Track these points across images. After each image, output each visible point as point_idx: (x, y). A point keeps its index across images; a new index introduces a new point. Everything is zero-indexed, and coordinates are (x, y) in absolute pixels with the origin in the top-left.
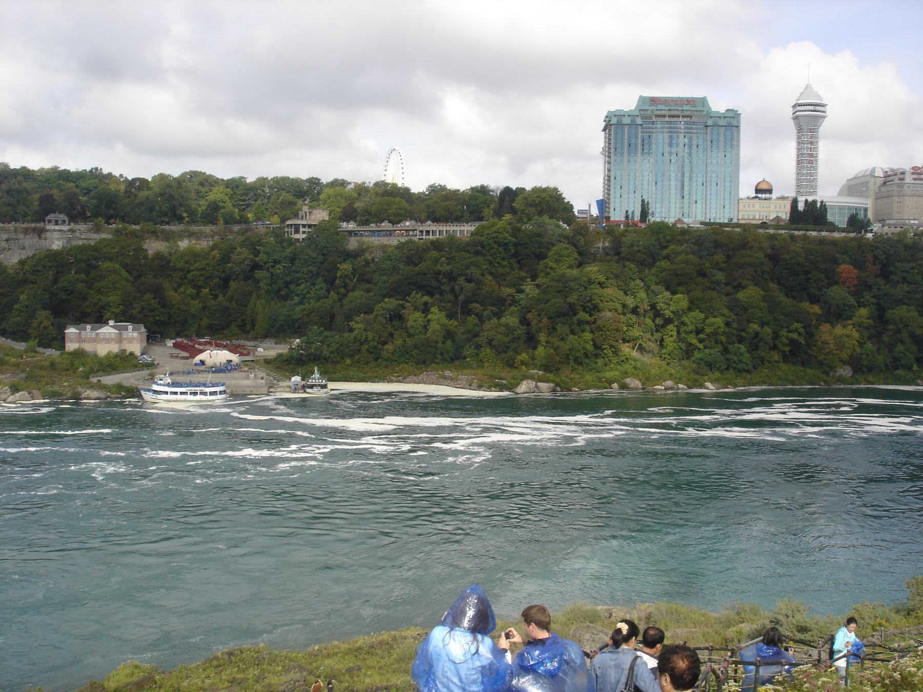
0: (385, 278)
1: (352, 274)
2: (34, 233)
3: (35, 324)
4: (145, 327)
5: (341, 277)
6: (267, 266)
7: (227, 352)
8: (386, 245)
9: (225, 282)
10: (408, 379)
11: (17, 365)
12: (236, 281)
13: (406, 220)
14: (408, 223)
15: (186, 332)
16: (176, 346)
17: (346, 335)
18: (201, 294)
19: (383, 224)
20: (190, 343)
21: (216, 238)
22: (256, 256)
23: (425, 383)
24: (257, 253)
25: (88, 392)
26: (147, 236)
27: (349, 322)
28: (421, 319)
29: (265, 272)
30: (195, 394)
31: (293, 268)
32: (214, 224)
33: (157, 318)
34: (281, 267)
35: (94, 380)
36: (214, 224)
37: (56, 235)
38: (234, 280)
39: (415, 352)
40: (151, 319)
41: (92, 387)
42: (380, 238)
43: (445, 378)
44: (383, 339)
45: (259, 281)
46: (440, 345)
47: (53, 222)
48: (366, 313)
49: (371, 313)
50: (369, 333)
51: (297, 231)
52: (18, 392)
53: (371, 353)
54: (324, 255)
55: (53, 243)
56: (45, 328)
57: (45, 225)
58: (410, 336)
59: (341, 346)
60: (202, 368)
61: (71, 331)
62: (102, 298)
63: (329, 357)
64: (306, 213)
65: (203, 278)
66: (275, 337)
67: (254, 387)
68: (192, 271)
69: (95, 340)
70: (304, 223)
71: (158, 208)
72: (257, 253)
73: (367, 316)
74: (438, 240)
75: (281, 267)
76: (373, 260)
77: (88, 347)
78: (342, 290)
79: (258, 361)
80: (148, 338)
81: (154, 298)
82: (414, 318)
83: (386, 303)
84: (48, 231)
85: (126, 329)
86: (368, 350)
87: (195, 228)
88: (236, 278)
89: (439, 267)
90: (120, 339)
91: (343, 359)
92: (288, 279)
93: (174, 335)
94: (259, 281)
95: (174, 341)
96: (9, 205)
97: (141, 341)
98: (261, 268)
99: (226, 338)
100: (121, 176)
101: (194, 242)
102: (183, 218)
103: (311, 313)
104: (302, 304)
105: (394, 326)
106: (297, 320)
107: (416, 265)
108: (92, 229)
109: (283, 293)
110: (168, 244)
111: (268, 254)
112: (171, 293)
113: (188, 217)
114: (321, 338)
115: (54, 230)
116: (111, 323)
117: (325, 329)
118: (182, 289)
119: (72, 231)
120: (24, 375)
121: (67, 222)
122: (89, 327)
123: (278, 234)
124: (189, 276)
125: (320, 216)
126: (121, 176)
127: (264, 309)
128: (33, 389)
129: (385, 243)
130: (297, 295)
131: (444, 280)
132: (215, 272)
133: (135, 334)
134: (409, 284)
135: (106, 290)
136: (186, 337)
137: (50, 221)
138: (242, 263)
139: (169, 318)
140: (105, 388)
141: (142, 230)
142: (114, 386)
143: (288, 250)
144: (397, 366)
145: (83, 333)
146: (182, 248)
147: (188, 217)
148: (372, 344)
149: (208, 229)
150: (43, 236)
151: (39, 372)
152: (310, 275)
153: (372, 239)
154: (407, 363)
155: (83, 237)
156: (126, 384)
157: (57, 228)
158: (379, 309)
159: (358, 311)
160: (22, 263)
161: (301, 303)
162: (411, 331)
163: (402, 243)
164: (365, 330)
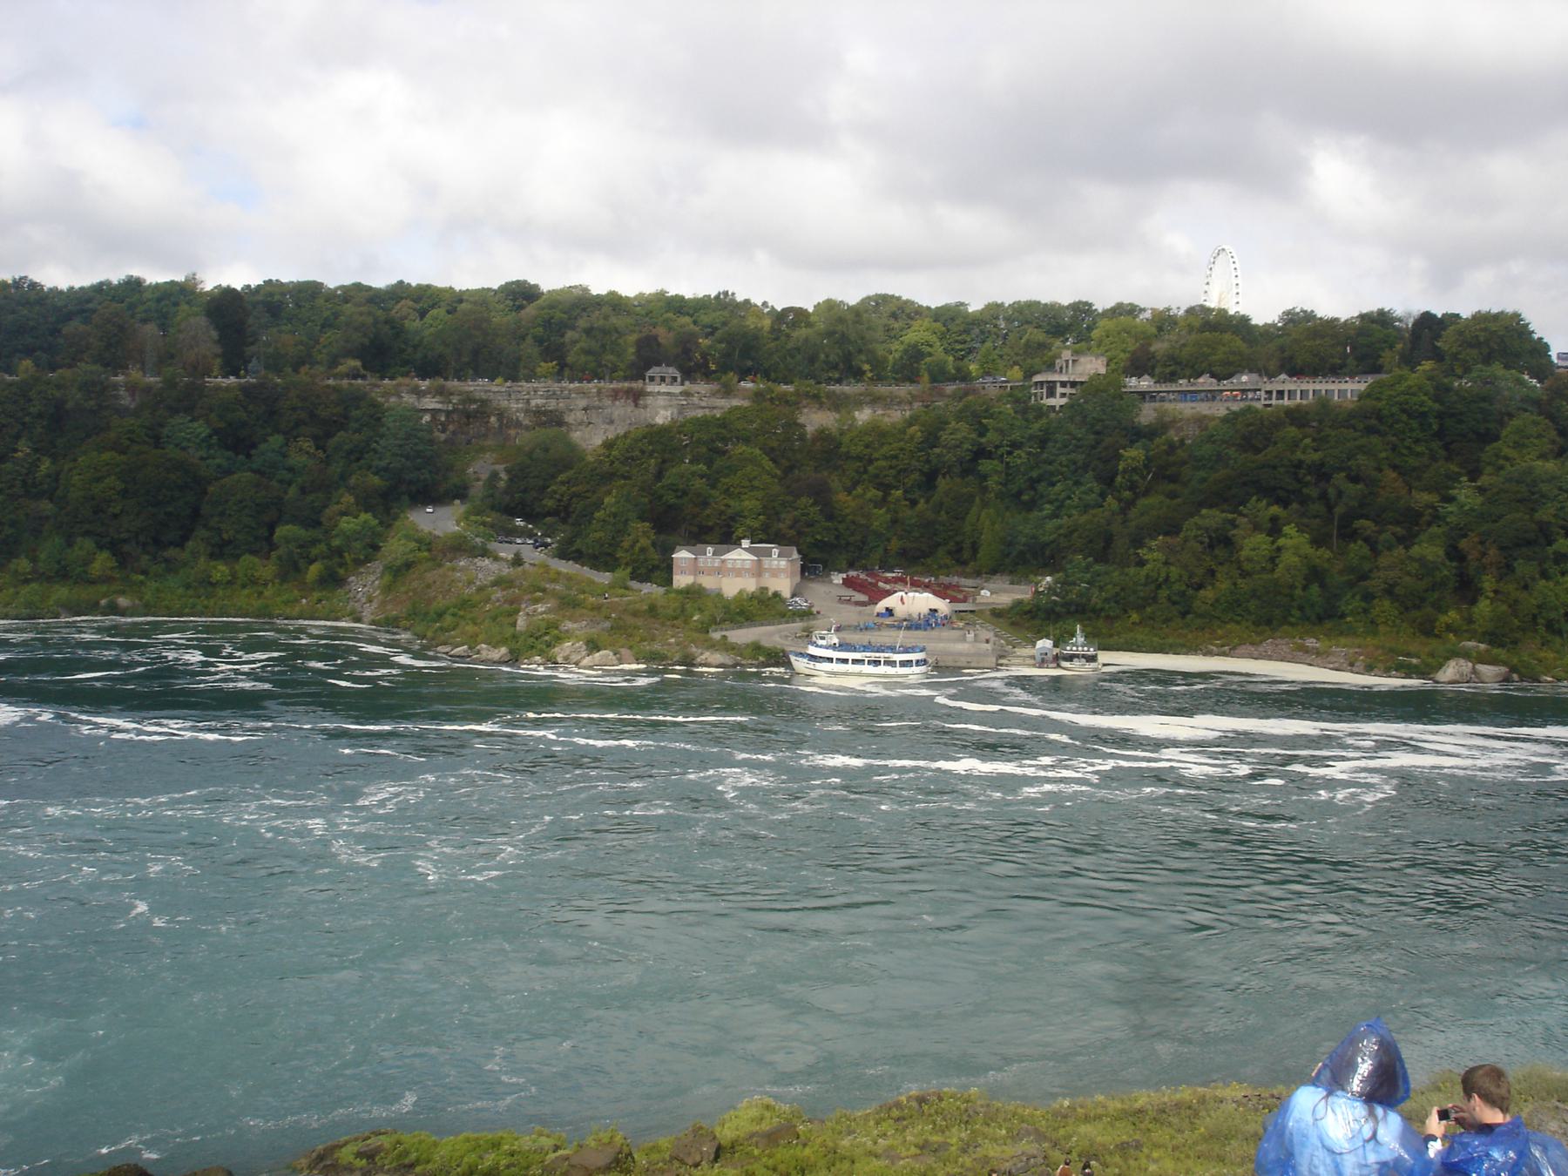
0: (1202, 474)
1: (1146, 466)
2: (627, 398)
3: (626, 544)
4: (799, 552)
5: (1125, 471)
6: (999, 453)
7: (931, 595)
8: (1205, 416)
9: (929, 480)
10: (1241, 650)
11: (597, 608)
12: (948, 476)
13: (1242, 373)
14: (1244, 378)
16: (848, 583)
17: (1132, 570)
18: (890, 499)
19: (1201, 380)
20: (869, 580)
21: (916, 405)
22: (982, 435)
23: (1270, 658)
25: (707, 654)
26: (805, 402)
28: (1265, 546)
29: (996, 462)
30: (876, 663)
31: (1045, 455)
32: (914, 382)
33: (818, 537)
34: (1023, 455)
35: (716, 636)
36: (912, 381)
37: (661, 401)
38: (944, 478)
39: (1253, 605)
40: (809, 539)
41: (713, 646)
42: (1193, 405)
43: (1306, 651)
44: (1196, 580)
45: (984, 477)
46: (1298, 592)
47: (658, 379)
48: (1166, 534)
49: (1177, 533)
50: (1172, 568)
51: (1051, 394)
52: (599, 651)
53: (1174, 603)
54: (1097, 433)
55: (657, 413)
56: (643, 550)
57: (645, 384)
58: (1245, 574)
59: (1123, 589)
60: (888, 621)
61: (682, 555)
62: (732, 503)
63: (1102, 609)
64: (1067, 361)
65: (893, 472)
66: (1011, 572)
68: (877, 459)
69: (720, 571)
70: (1065, 378)
71: (822, 356)
73: (1168, 539)
74: (1299, 406)
75: (1023, 455)
76: (1182, 441)
77: (708, 582)
78: (1127, 494)
79: (981, 611)
80: (803, 569)
81: (812, 505)
82: (1254, 545)
83: (1202, 517)
84: (650, 394)
86: (1169, 599)
87: (882, 389)
88: (948, 472)
89: (1299, 455)
90: (758, 571)
91: (1125, 611)
92: (1034, 474)
93: (844, 565)
94: (984, 477)
95: (844, 576)
96: (588, 352)
97: (792, 574)
98: (990, 456)
99: (930, 573)
100: (765, 304)
101: (880, 412)
102: (864, 373)
103: (1071, 533)
105: (1216, 557)
106: (1048, 545)
107: (1258, 451)
108: (718, 391)
109: (1025, 497)
110: (837, 416)
111: (1001, 431)
113: (871, 371)
114: (1088, 575)
115: (659, 393)
116: (746, 543)
117: (1096, 561)
118: (859, 490)
119: (687, 394)
120: (607, 624)
121: (679, 380)
122: (710, 549)
123: (1019, 399)
124: (870, 468)
125: (1091, 366)
126: (765, 304)
127: (993, 523)
129: (1205, 412)
130: (1050, 502)
131: (1309, 478)
132: (914, 463)
133: (783, 563)
134: (1245, 484)
135: (737, 491)
136: (864, 568)
137: (652, 379)
138: (958, 447)
139: (837, 537)
140: (733, 649)
141: (797, 393)
143: (1036, 426)
144: (1220, 627)
145: (701, 559)
146: (860, 423)
147: (871, 371)
148: (1176, 587)
149: (903, 390)
151: (630, 620)
152: (1072, 467)
153: (1180, 406)
154: (1238, 623)
155: (703, 404)
156: (766, 643)
157: (663, 388)
158: (1190, 527)
159: (1154, 530)
160: (609, 445)
161: (1055, 515)
162: (1247, 566)
163: (1234, 413)
164: (1166, 563)
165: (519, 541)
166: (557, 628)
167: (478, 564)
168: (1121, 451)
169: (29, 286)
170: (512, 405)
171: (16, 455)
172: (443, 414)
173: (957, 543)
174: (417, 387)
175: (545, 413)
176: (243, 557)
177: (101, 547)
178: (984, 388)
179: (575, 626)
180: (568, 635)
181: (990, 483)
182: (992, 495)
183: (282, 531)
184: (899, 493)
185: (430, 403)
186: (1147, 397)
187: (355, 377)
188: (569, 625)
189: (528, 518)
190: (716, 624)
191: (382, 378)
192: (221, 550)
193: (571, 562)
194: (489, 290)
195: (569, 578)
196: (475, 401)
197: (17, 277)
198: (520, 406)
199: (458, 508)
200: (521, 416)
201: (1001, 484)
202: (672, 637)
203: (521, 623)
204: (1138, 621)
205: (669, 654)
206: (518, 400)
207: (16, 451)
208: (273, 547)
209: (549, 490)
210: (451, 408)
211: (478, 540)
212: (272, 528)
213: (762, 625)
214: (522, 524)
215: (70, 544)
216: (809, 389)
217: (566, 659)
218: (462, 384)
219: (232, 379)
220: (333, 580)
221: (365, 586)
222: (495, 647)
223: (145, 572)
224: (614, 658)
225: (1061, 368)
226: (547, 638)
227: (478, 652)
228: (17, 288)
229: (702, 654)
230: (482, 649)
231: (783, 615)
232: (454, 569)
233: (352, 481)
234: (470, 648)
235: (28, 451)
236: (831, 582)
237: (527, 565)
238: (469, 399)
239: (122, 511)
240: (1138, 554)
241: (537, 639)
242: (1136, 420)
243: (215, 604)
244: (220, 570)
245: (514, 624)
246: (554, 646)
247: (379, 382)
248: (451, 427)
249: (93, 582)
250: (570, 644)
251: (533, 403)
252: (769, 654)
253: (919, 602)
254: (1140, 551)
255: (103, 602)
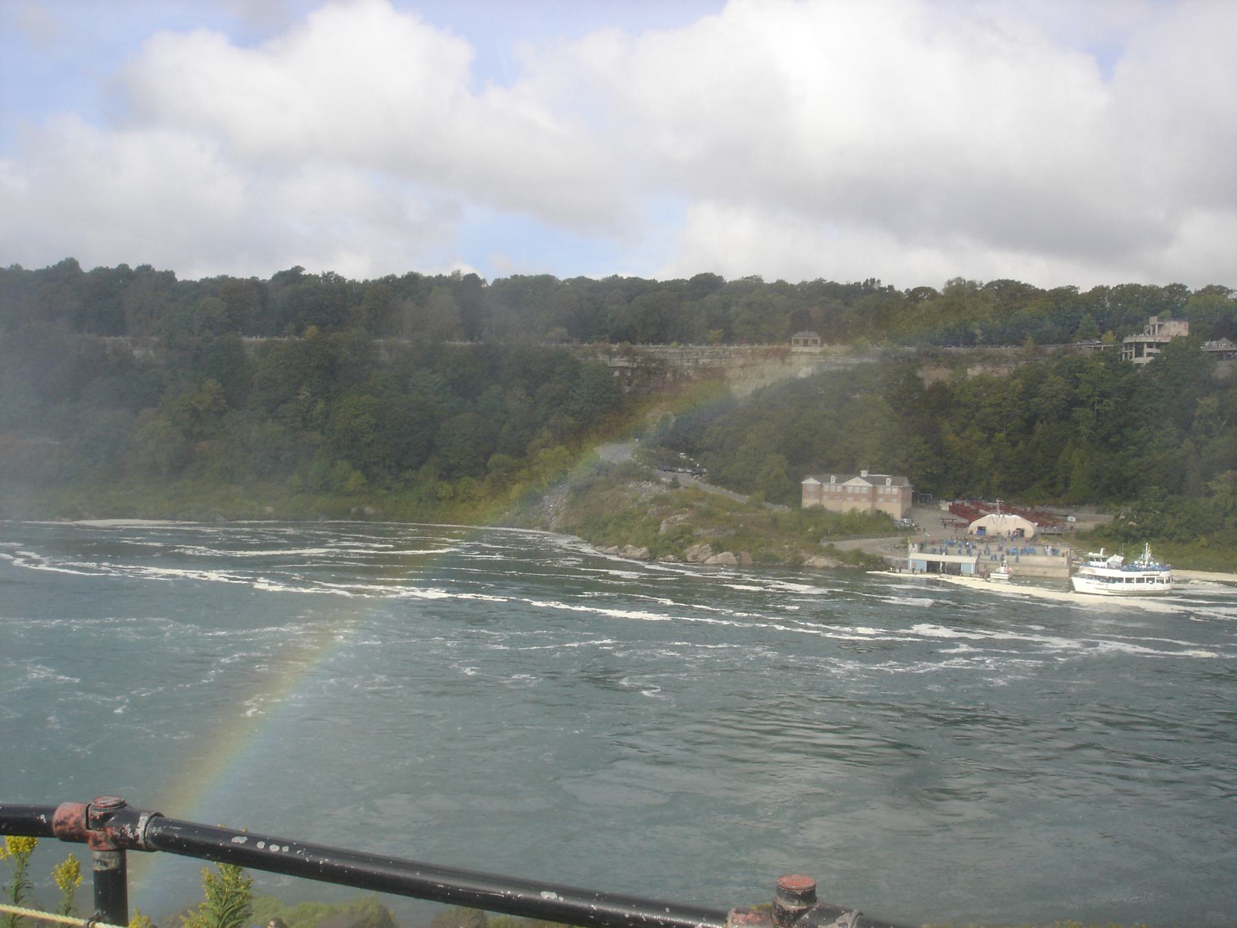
4: (911, 482)
5: (1201, 417)
7: (1018, 517)
9: (1030, 423)
12: (1045, 422)
15: (969, 493)
16: (953, 510)
18: (993, 440)
20: (973, 507)
21: (1022, 364)
22: (1077, 387)
24: (1076, 383)
25: (814, 558)
27: (1208, 481)
32: (1021, 345)
33: (929, 471)
34: (1112, 403)
35: (825, 544)
36: (1017, 344)
37: (804, 359)
38: (1042, 422)
41: (820, 552)
45: (1078, 423)
47: (801, 342)
52: (722, 552)
59: (1194, 516)
61: (810, 482)
63: (1174, 533)
64: (1154, 326)
65: (997, 417)
67: (1050, 567)
69: (843, 495)
70: (1151, 340)
72: (1076, 383)
77: (831, 505)
78: (1203, 437)
81: (925, 442)
84: (794, 353)
85: (883, 482)
87: (990, 350)
90: (873, 496)
95: (951, 504)
97: (904, 500)
98: (1082, 404)
101: (989, 369)
102: (977, 336)
104: (1140, 456)
109: (1112, 440)
112: (951, 437)
113: (982, 335)
115: (802, 353)
116: (864, 473)
117: (1171, 492)
118: (967, 433)
120: (733, 532)
121: (819, 342)
122: (833, 478)
124: (977, 415)
125: (1177, 329)
127: (1082, 462)
128: (743, 550)
130: (1135, 444)
133: (895, 490)
136: (970, 499)
137: (797, 342)
138: (1054, 397)
140: (838, 554)
142: (850, 553)
143: (1124, 379)
146: (971, 378)
149: (1008, 350)
150: (787, 360)
156: (867, 552)
157: (806, 350)
160: (757, 394)
165: (680, 470)
166: (690, 532)
167: (643, 486)
168: (1197, 399)
169: (334, 279)
170: (684, 364)
171: (299, 397)
172: (630, 371)
173: (1051, 478)
174: (610, 349)
175: (711, 370)
176: (464, 478)
177: (355, 468)
178: (1081, 349)
179: (705, 532)
180: (699, 538)
181: (1082, 427)
182: (1084, 438)
183: (494, 459)
184: (1002, 435)
185: (620, 362)
186: (1224, 356)
187: (562, 341)
188: (701, 531)
189: (690, 451)
190: (827, 535)
191: (583, 342)
192: (448, 473)
193: (719, 487)
194: (682, 280)
195: (714, 498)
196: (655, 361)
197: (326, 272)
198: (690, 364)
199: (635, 443)
200: (691, 372)
201: (1092, 428)
202: (787, 544)
203: (663, 527)
204: (1206, 545)
205: (782, 557)
206: (688, 360)
207: (299, 394)
208: (488, 471)
209: (708, 430)
210: (635, 366)
211: (645, 467)
212: (487, 456)
213: (867, 537)
214: (684, 457)
215: (332, 466)
216: (928, 349)
217: (695, 557)
218: (645, 346)
219: (468, 343)
220: (533, 499)
221: (555, 503)
222: (639, 547)
223: (388, 489)
224: (734, 558)
225: (1149, 333)
226: (681, 541)
227: (625, 551)
228: (326, 281)
229: (810, 558)
230: (628, 548)
231: (886, 530)
232: (623, 490)
233: (552, 421)
234: (619, 548)
235: (308, 394)
236: (939, 509)
237: (682, 488)
238: (650, 358)
239: (373, 441)
240: (1207, 486)
241: (673, 541)
242: (1213, 375)
243: (439, 514)
244: (445, 488)
245: (657, 531)
246: (685, 548)
247: (580, 345)
248: (635, 382)
249: (348, 495)
250: (698, 546)
251: (701, 362)
252: (869, 560)
253: (1012, 522)
254: (1209, 483)
255: (354, 510)
